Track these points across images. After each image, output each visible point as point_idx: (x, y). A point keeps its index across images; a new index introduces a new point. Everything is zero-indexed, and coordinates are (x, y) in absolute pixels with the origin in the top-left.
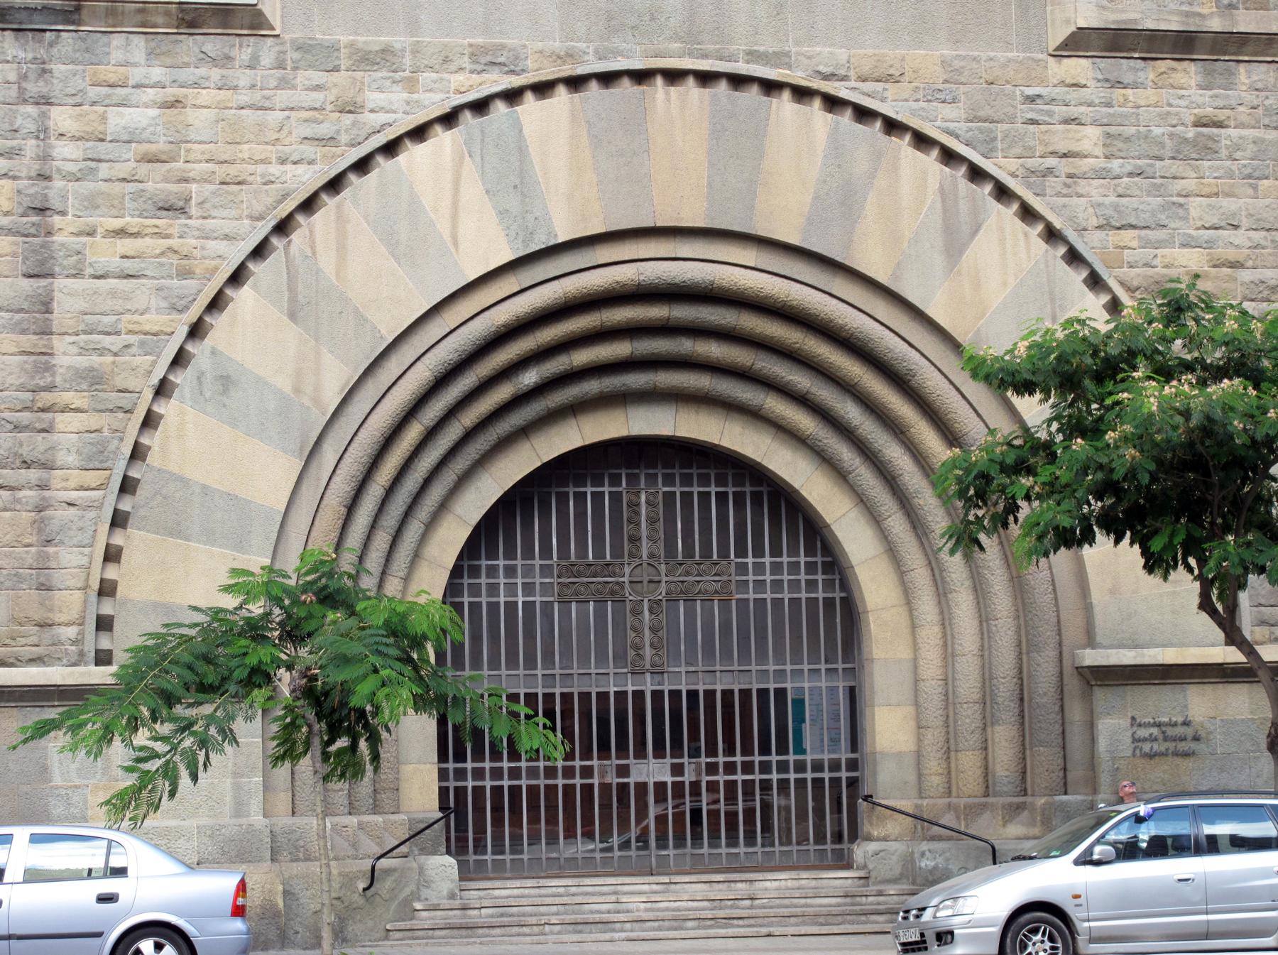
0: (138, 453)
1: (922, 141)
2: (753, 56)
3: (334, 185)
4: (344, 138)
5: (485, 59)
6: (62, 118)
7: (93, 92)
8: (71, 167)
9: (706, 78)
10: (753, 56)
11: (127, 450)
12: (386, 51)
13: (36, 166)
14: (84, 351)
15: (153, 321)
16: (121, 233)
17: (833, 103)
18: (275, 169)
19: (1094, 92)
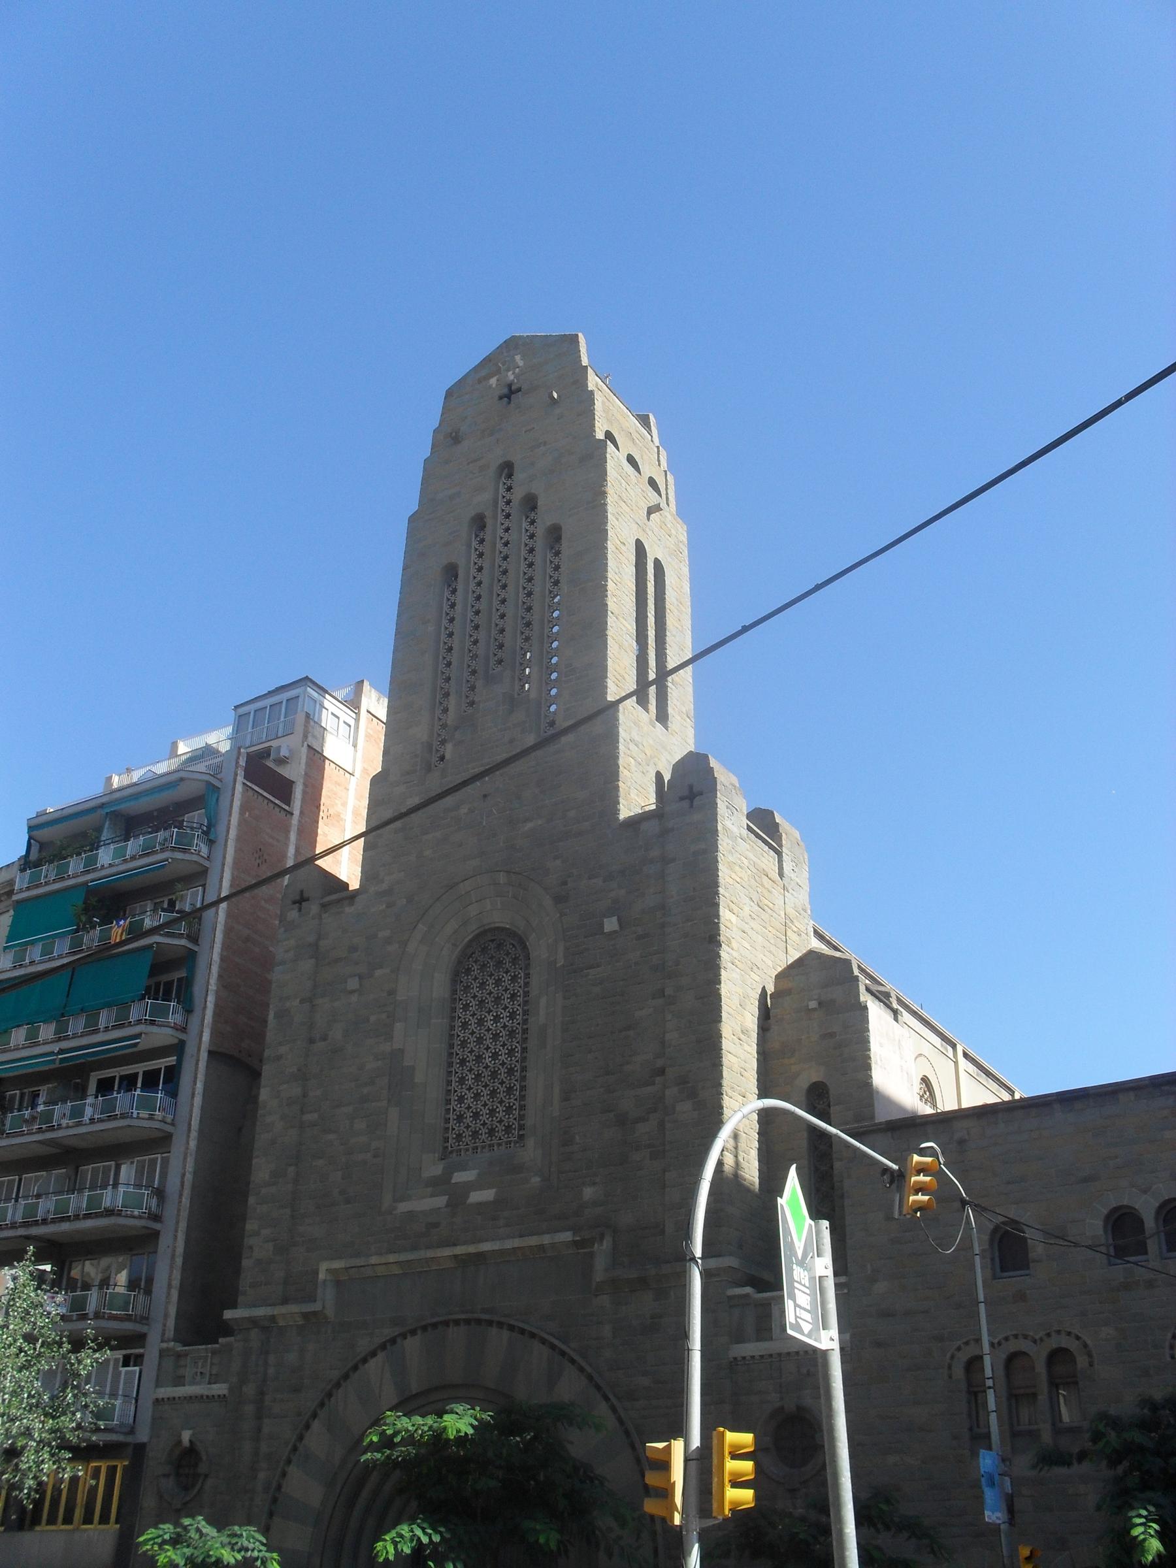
9: (468, 1322)
17: (512, 1328)
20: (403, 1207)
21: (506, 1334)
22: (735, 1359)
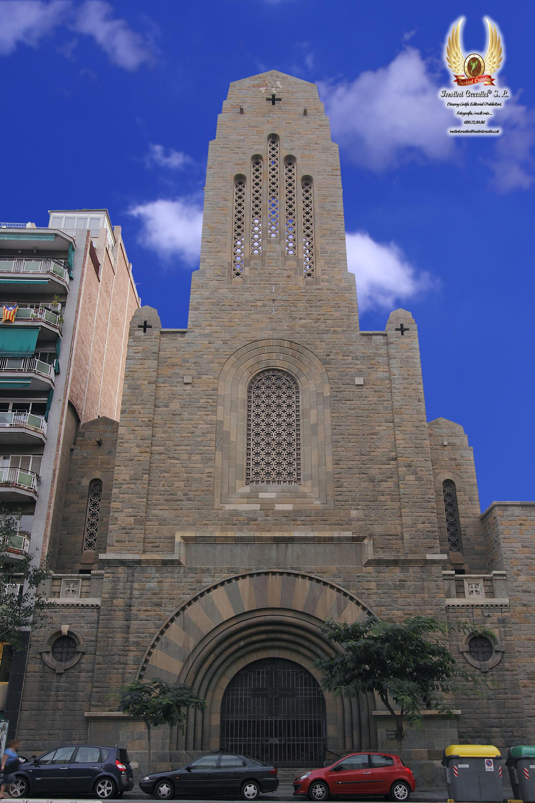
0: (146, 661)
1: (332, 587)
2: (292, 568)
3: (195, 599)
4: (198, 589)
5: (230, 570)
6: (136, 585)
7: (143, 579)
8: (137, 596)
9: (281, 574)
10: (292, 568)
11: (143, 660)
12: (208, 569)
13: (129, 596)
14: (136, 637)
15: (152, 630)
16: (146, 611)
17: (311, 579)
18: (181, 596)
19: (374, 574)
20: (228, 507)
21: (308, 582)
22: (449, 606)
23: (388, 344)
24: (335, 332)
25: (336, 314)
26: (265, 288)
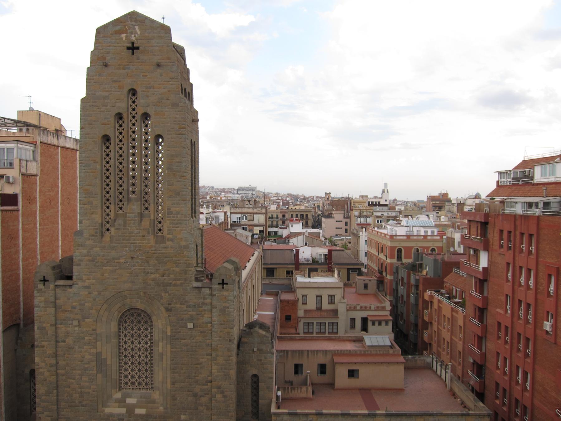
23: (212, 295)
24: (175, 285)
25: (177, 269)
26: (126, 246)
